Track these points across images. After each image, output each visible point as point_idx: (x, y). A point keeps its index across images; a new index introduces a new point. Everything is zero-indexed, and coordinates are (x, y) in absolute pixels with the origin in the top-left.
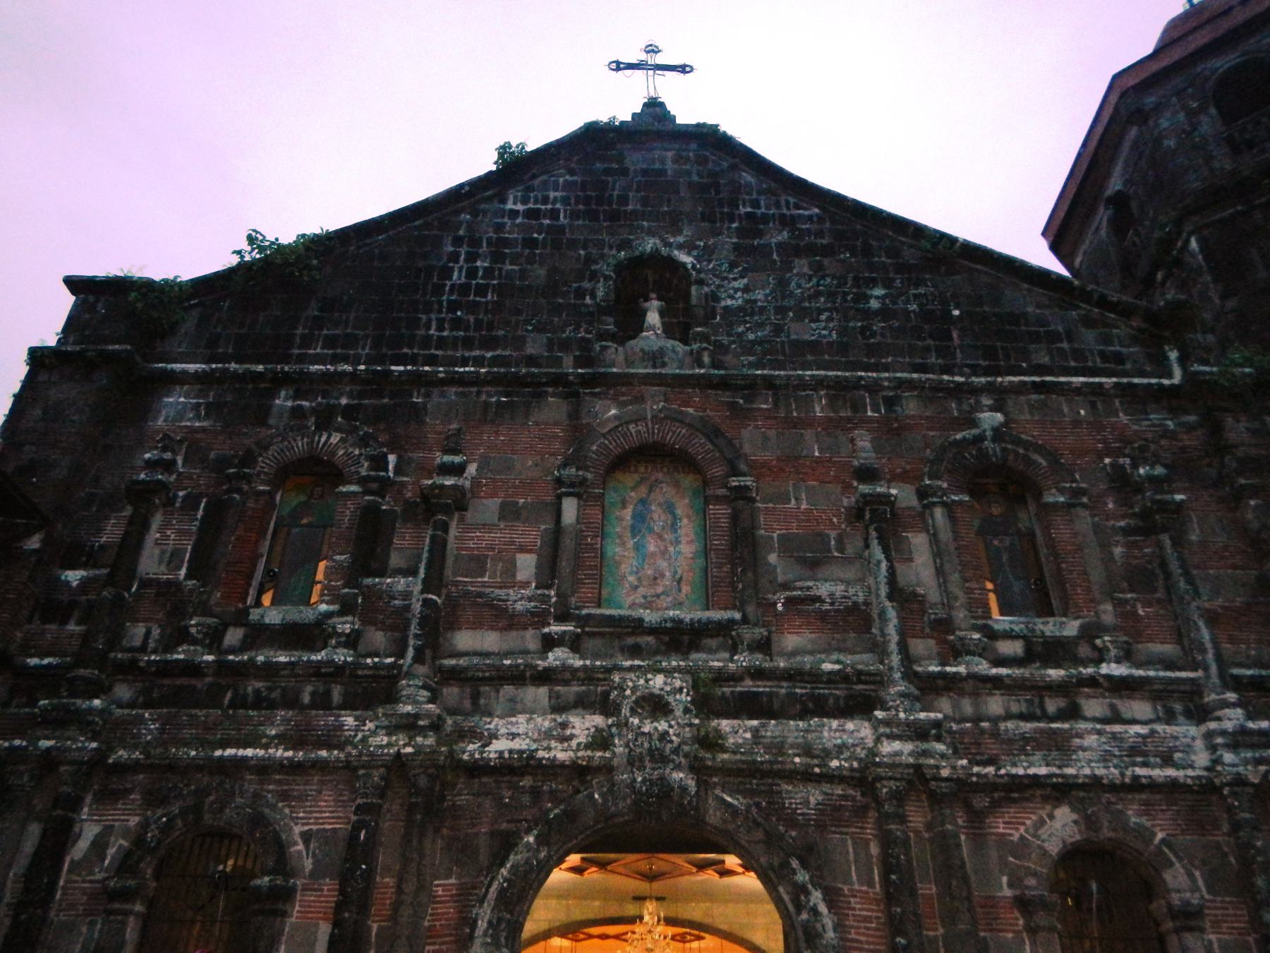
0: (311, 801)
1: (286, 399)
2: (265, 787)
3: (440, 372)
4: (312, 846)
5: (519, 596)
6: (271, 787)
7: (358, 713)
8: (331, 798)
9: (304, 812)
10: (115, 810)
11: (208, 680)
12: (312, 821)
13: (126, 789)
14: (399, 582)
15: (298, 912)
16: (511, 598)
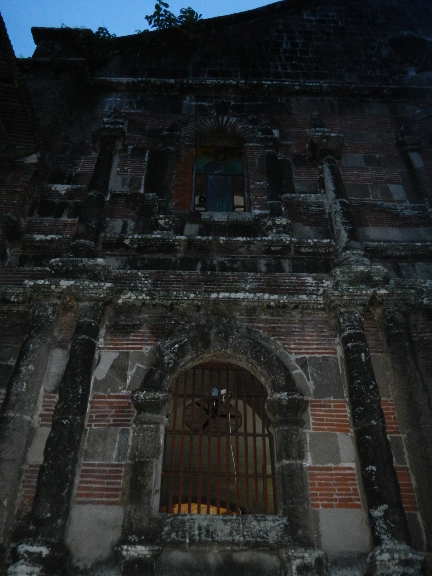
0: (297, 335)
1: (191, 101)
2: (256, 325)
3: (297, 85)
4: (309, 371)
5: (403, 207)
6: (260, 325)
7: (314, 275)
8: (315, 334)
9: (294, 344)
10: (127, 340)
11: (179, 255)
12: (303, 351)
13: (134, 325)
14: (311, 196)
15: (313, 424)
16: (398, 208)
